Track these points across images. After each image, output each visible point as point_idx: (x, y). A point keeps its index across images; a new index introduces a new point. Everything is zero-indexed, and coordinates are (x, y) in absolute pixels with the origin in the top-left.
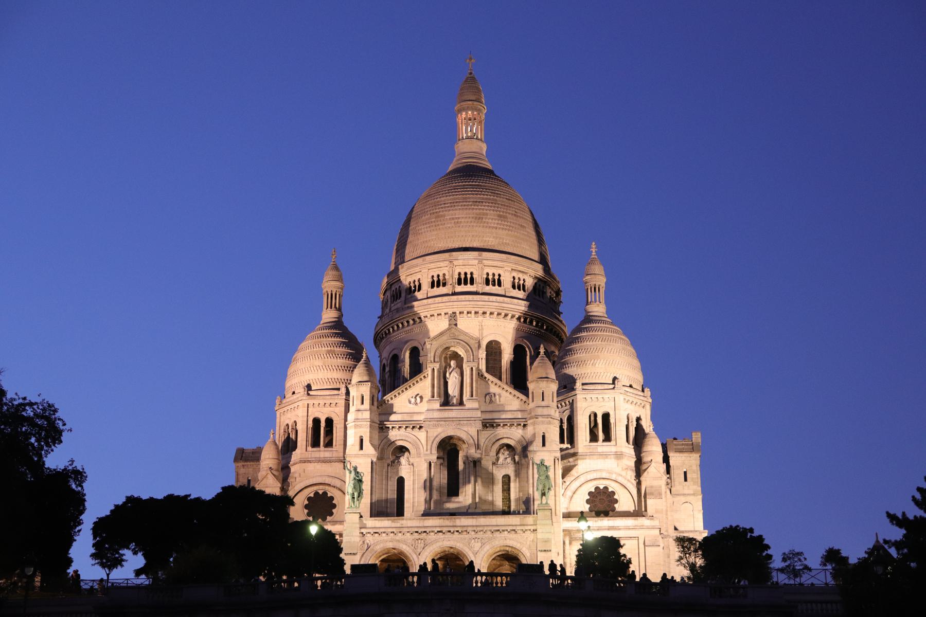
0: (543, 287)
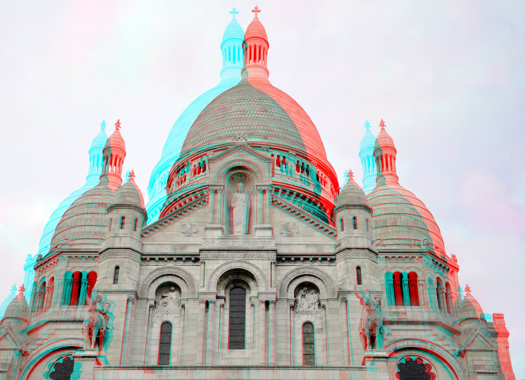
0: (325, 177)
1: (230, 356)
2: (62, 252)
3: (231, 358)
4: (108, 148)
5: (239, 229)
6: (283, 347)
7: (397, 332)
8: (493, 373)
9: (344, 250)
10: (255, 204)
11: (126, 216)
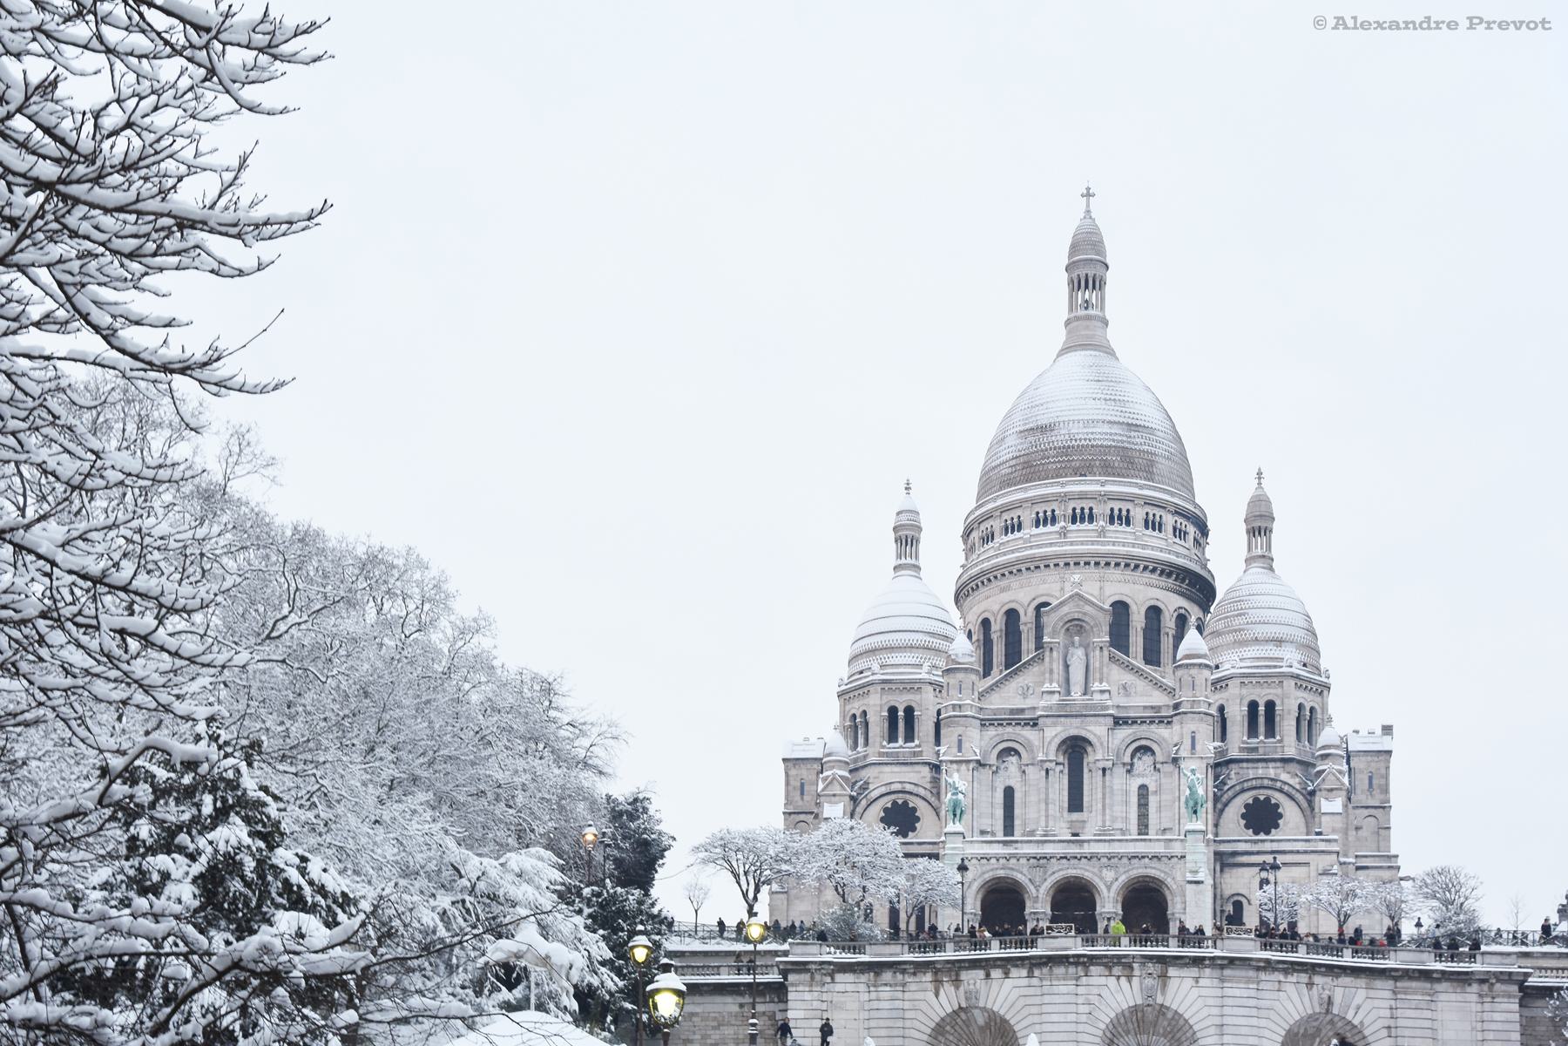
6: (1118, 810)
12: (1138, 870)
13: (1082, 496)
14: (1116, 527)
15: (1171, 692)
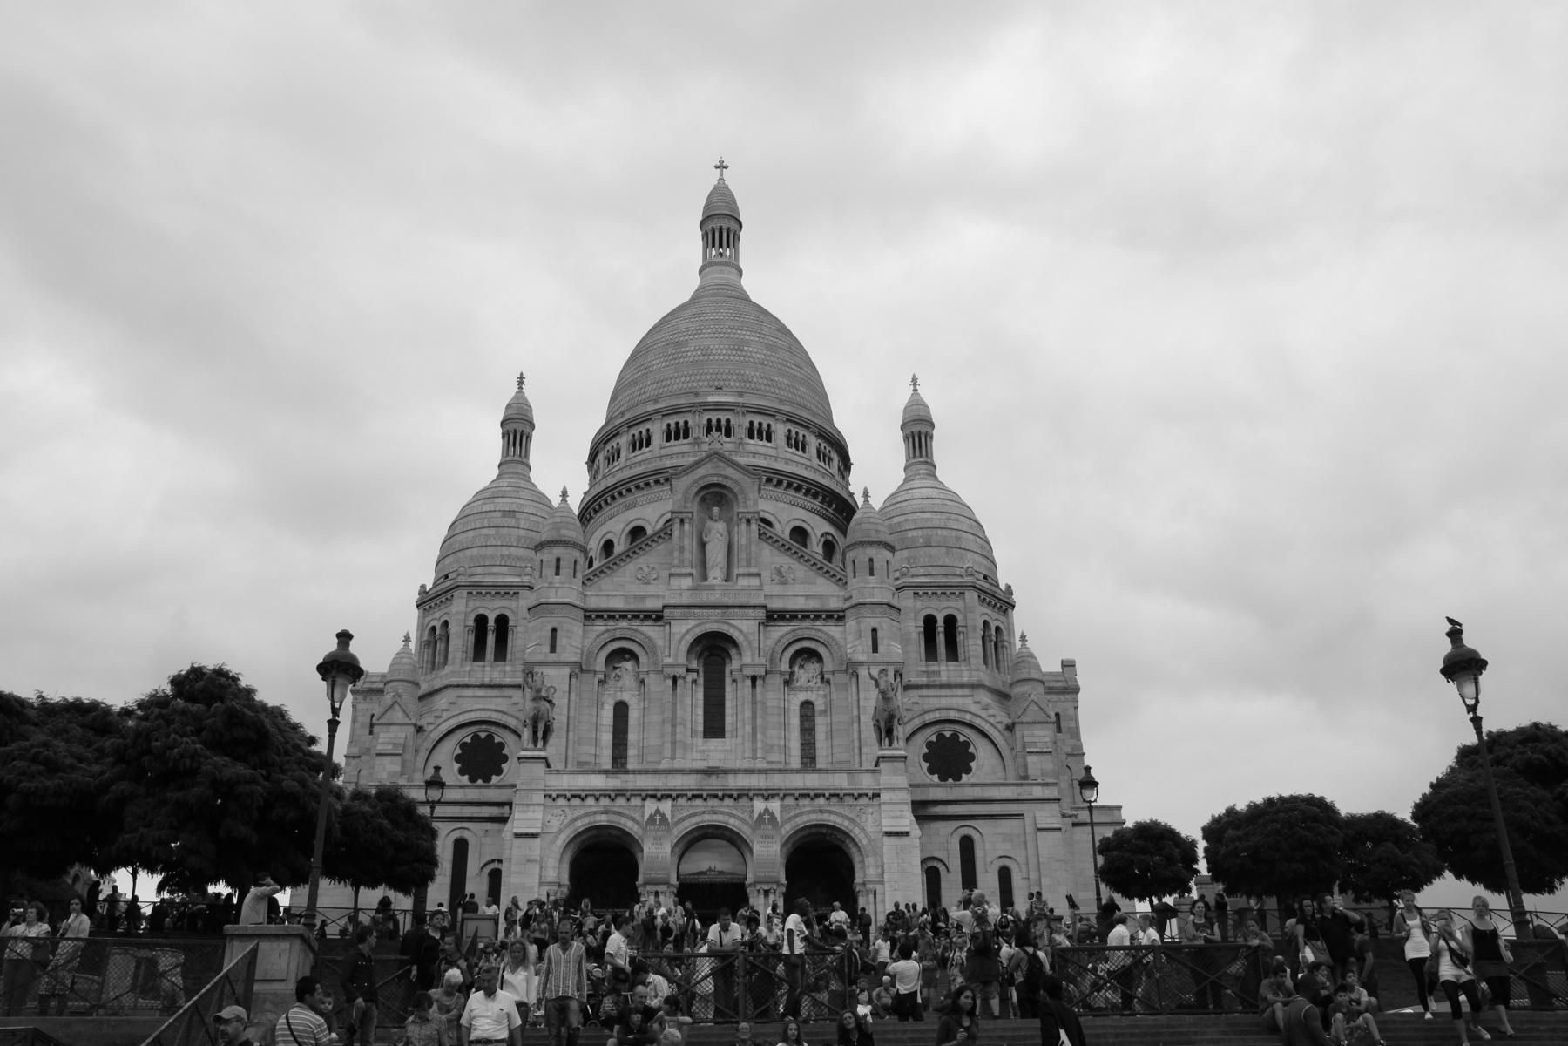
0: (830, 451)
1: (704, 748)
2: (458, 586)
3: (708, 751)
4: (509, 419)
5: (716, 575)
7: (926, 699)
8: (1046, 752)
9: (856, 605)
10: (736, 538)
11: (561, 556)
12: (809, 814)
13: (719, 407)
14: (756, 441)
15: (841, 582)
